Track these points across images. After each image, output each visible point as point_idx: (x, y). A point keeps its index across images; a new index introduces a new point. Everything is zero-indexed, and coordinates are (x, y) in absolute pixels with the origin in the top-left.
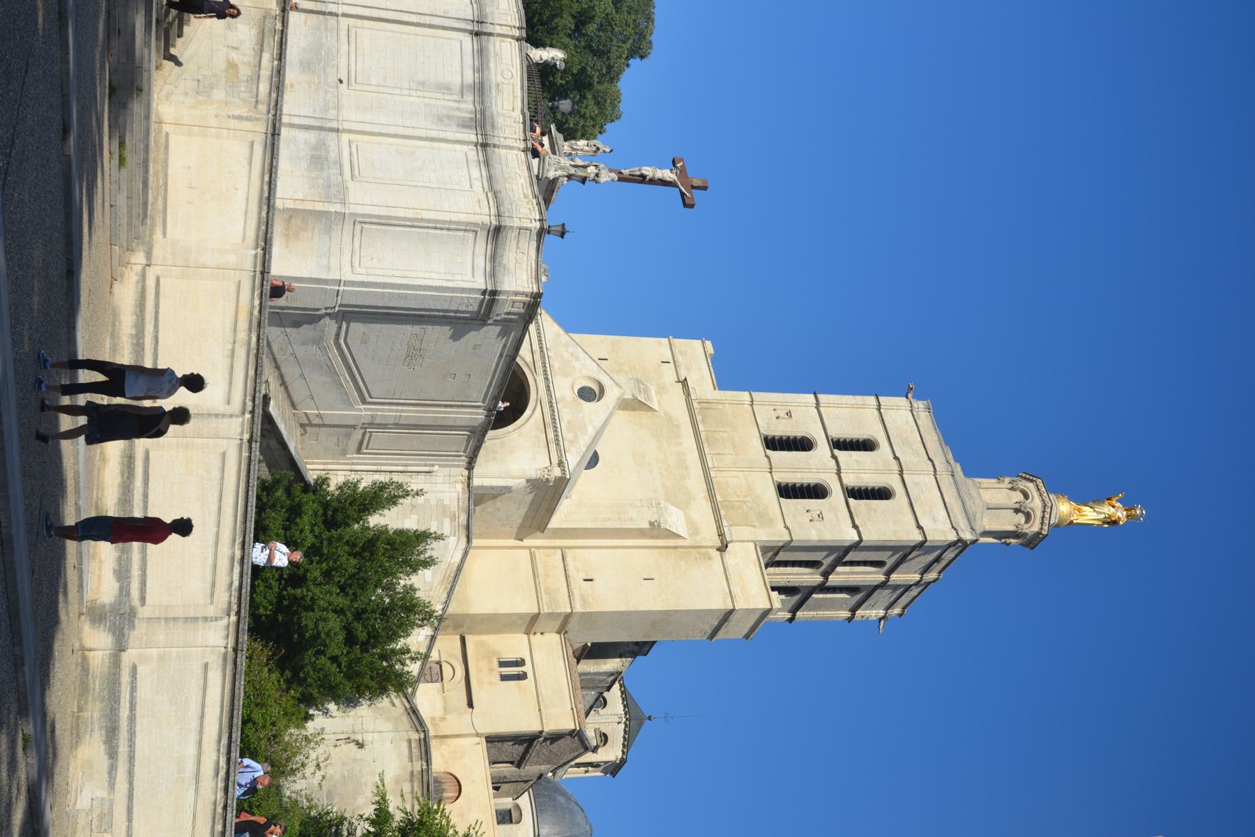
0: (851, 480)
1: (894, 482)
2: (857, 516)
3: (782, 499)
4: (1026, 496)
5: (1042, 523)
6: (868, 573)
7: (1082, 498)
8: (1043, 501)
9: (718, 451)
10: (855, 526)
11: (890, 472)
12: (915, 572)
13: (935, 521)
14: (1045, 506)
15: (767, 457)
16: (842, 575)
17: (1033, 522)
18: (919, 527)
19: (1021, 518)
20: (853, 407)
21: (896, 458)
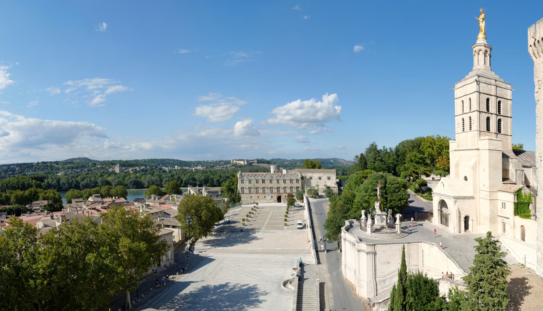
4: (475, 51)
5: (481, 46)
6: (491, 102)
10: (474, 111)
12: (491, 87)
16: (493, 108)
18: (474, 92)
19: (481, 53)
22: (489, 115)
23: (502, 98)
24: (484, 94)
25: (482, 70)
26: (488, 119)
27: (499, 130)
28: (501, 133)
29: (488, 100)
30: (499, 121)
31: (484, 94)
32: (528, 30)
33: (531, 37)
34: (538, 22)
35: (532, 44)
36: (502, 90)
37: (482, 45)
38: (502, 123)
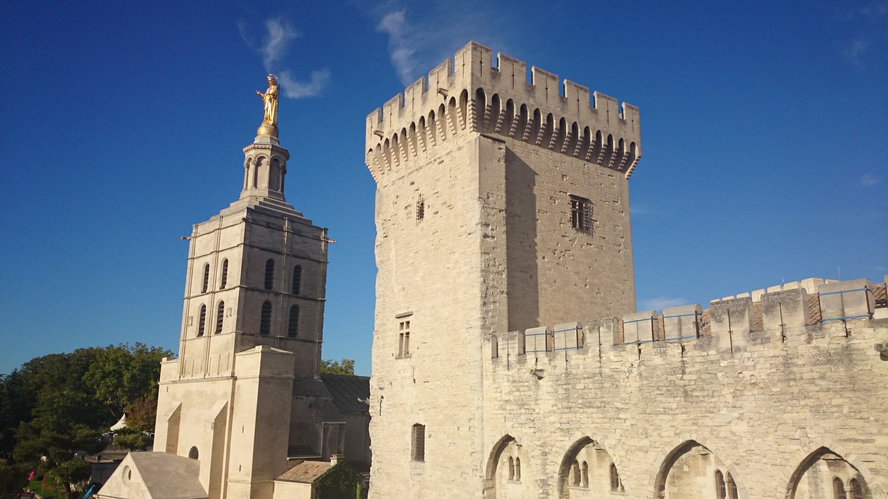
0: (218, 285)
1: (222, 256)
2: (232, 286)
3: (222, 333)
7: (259, 117)
8: (252, 149)
9: (200, 368)
10: (234, 288)
11: (217, 259)
13: (238, 235)
14: (254, 148)
15: (204, 337)
16: (282, 284)
17: (263, 154)
19: (265, 162)
20: (191, 275)
21: (211, 253)
22: (271, 298)
23: (303, 258)
24: (262, 249)
25: (262, 200)
26: (267, 308)
27: (292, 332)
28: (297, 338)
29: (270, 264)
30: (295, 310)
31: (262, 249)
32: (368, 119)
33: (372, 133)
34: (388, 103)
35: (374, 147)
36: (306, 243)
37: (268, 146)
38: (301, 313)
